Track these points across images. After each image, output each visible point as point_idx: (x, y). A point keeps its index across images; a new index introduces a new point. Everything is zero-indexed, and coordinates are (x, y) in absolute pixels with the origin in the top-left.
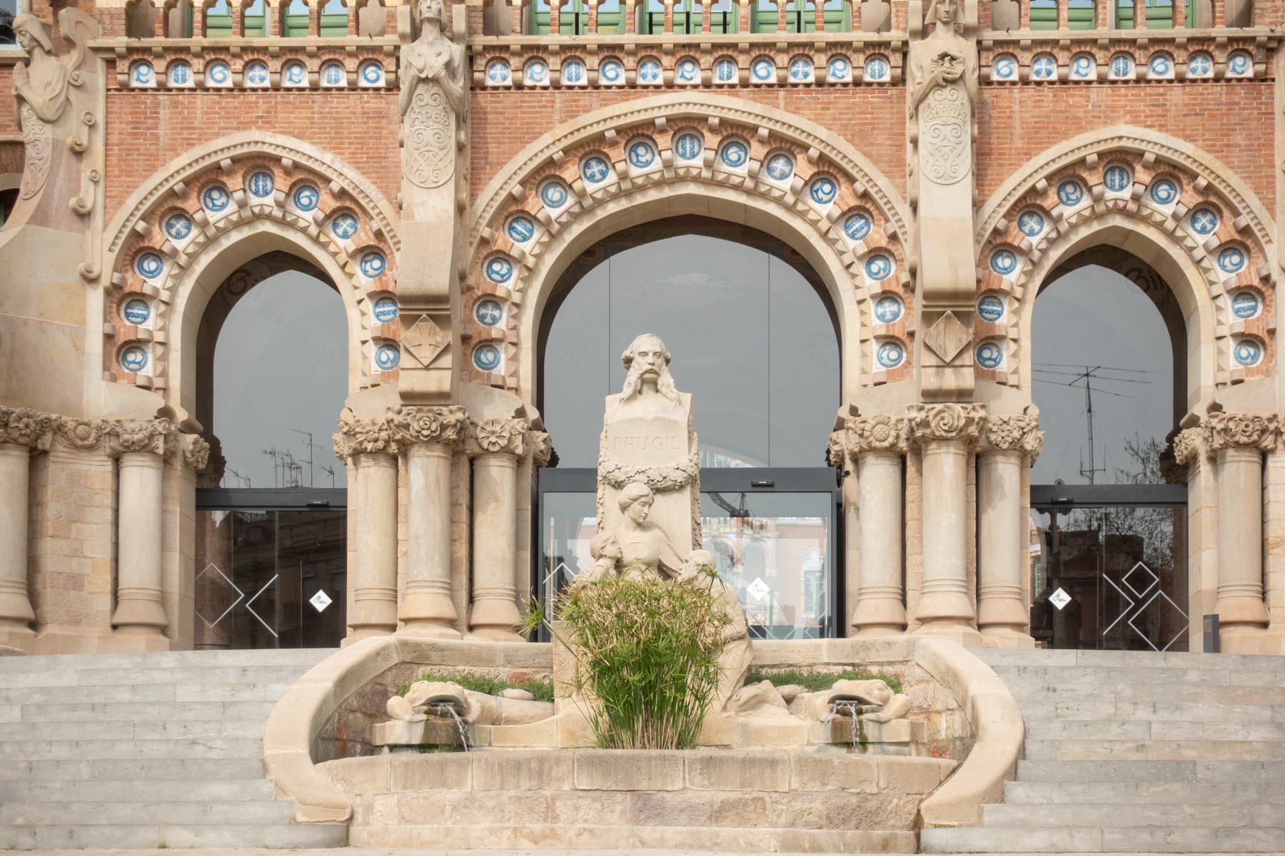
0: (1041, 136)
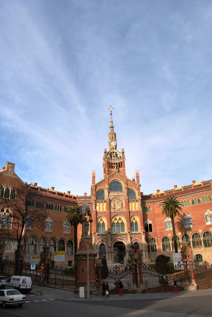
0: (133, 239)
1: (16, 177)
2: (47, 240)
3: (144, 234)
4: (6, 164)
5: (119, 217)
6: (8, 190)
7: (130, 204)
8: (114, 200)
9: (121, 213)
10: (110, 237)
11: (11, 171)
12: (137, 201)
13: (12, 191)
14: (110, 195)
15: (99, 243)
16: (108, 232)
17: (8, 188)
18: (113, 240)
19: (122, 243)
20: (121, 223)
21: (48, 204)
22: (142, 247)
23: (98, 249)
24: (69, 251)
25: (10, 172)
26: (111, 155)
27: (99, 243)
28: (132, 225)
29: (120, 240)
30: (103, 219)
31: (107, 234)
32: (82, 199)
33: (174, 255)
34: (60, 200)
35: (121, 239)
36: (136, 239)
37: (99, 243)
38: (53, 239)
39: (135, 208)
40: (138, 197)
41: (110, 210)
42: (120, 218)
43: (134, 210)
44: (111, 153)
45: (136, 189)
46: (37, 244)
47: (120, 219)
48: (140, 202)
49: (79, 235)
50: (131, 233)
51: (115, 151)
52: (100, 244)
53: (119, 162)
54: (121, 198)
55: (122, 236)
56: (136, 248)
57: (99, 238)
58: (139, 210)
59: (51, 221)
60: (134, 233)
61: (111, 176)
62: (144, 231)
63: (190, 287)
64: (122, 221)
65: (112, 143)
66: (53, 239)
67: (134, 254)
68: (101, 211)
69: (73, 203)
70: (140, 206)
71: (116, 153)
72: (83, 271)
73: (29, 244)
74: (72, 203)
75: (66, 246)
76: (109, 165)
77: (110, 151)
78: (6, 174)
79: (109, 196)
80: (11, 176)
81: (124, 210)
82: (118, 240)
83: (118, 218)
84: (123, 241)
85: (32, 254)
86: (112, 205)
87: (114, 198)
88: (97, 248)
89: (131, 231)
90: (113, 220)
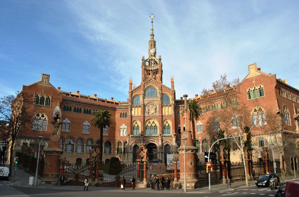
0: (164, 141)
1: (50, 86)
2: (84, 141)
3: (175, 136)
4: (41, 75)
5: (153, 121)
6: (43, 98)
7: (163, 109)
8: (148, 105)
9: (154, 117)
10: (142, 138)
11: (46, 81)
12: (170, 105)
13: (46, 98)
14: (145, 100)
15: (132, 144)
16: (141, 134)
17: (43, 96)
18: (146, 142)
19: (155, 145)
20: (154, 126)
21: (86, 109)
22: (172, 148)
23: (132, 149)
24: (107, 151)
25: (45, 83)
26: (149, 62)
27: (132, 144)
28: (164, 128)
29: (152, 142)
30: (138, 122)
31: (140, 136)
32: (123, 104)
33: (168, 156)
34: (98, 106)
35: (153, 141)
36: (167, 142)
37: (133, 144)
38: (91, 140)
39: (168, 112)
40: (172, 102)
41: (144, 114)
42: (153, 122)
43: (167, 114)
44: (150, 60)
45: (170, 94)
46: (74, 144)
47: (153, 122)
48: (172, 107)
49: (117, 137)
50: (162, 136)
51: (153, 58)
52: (133, 145)
53: (156, 69)
54: (155, 103)
55: (154, 139)
56: (96, 147)
57: (133, 140)
58: (171, 114)
59: (89, 124)
60: (166, 135)
61: (146, 82)
62: (175, 134)
63: (139, 184)
64: (156, 124)
65: (151, 51)
66: (81, 140)
67: (93, 153)
68: (136, 116)
69: (112, 108)
70: (173, 111)
71: (154, 60)
72: (46, 165)
73: (66, 144)
74: (110, 108)
75: (103, 146)
76: (146, 71)
77: (149, 58)
78: (41, 84)
79: (143, 101)
80: (46, 86)
81: (158, 114)
82: (150, 141)
83: (151, 121)
84: (155, 143)
85: (70, 152)
86: (147, 110)
87: (149, 103)
88: (131, 149)
89: (162, 134)
90: (147, 123)
